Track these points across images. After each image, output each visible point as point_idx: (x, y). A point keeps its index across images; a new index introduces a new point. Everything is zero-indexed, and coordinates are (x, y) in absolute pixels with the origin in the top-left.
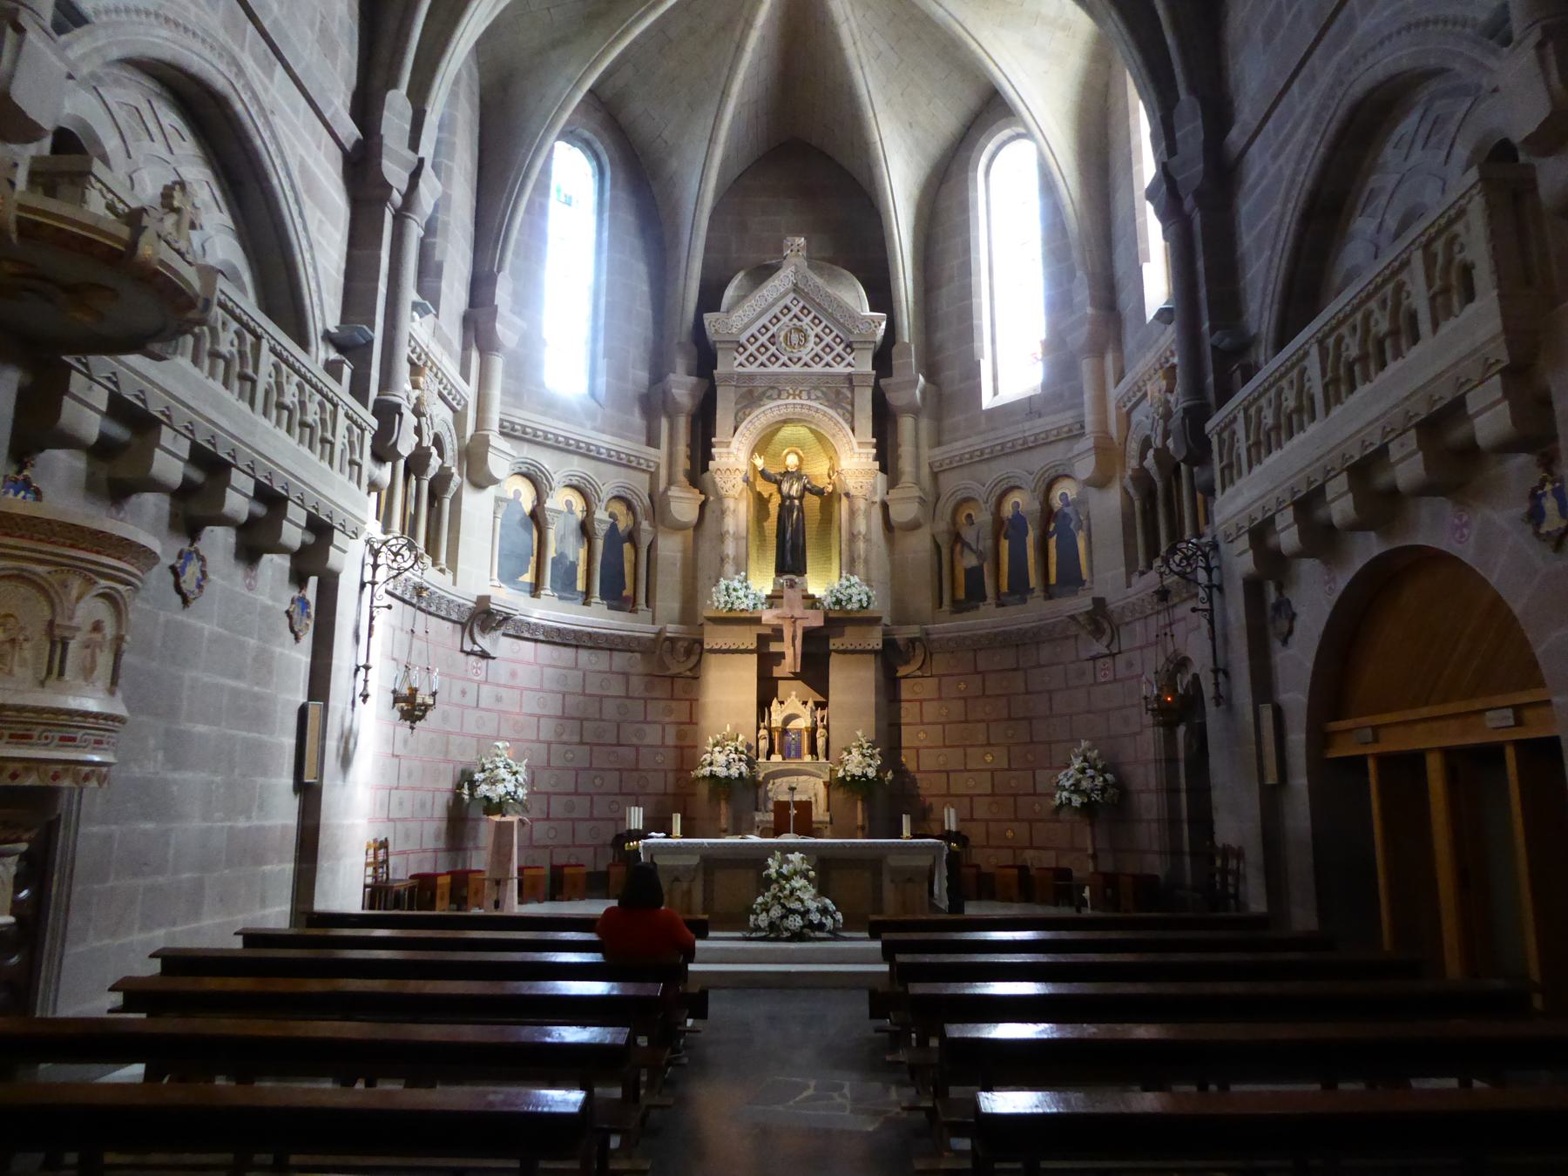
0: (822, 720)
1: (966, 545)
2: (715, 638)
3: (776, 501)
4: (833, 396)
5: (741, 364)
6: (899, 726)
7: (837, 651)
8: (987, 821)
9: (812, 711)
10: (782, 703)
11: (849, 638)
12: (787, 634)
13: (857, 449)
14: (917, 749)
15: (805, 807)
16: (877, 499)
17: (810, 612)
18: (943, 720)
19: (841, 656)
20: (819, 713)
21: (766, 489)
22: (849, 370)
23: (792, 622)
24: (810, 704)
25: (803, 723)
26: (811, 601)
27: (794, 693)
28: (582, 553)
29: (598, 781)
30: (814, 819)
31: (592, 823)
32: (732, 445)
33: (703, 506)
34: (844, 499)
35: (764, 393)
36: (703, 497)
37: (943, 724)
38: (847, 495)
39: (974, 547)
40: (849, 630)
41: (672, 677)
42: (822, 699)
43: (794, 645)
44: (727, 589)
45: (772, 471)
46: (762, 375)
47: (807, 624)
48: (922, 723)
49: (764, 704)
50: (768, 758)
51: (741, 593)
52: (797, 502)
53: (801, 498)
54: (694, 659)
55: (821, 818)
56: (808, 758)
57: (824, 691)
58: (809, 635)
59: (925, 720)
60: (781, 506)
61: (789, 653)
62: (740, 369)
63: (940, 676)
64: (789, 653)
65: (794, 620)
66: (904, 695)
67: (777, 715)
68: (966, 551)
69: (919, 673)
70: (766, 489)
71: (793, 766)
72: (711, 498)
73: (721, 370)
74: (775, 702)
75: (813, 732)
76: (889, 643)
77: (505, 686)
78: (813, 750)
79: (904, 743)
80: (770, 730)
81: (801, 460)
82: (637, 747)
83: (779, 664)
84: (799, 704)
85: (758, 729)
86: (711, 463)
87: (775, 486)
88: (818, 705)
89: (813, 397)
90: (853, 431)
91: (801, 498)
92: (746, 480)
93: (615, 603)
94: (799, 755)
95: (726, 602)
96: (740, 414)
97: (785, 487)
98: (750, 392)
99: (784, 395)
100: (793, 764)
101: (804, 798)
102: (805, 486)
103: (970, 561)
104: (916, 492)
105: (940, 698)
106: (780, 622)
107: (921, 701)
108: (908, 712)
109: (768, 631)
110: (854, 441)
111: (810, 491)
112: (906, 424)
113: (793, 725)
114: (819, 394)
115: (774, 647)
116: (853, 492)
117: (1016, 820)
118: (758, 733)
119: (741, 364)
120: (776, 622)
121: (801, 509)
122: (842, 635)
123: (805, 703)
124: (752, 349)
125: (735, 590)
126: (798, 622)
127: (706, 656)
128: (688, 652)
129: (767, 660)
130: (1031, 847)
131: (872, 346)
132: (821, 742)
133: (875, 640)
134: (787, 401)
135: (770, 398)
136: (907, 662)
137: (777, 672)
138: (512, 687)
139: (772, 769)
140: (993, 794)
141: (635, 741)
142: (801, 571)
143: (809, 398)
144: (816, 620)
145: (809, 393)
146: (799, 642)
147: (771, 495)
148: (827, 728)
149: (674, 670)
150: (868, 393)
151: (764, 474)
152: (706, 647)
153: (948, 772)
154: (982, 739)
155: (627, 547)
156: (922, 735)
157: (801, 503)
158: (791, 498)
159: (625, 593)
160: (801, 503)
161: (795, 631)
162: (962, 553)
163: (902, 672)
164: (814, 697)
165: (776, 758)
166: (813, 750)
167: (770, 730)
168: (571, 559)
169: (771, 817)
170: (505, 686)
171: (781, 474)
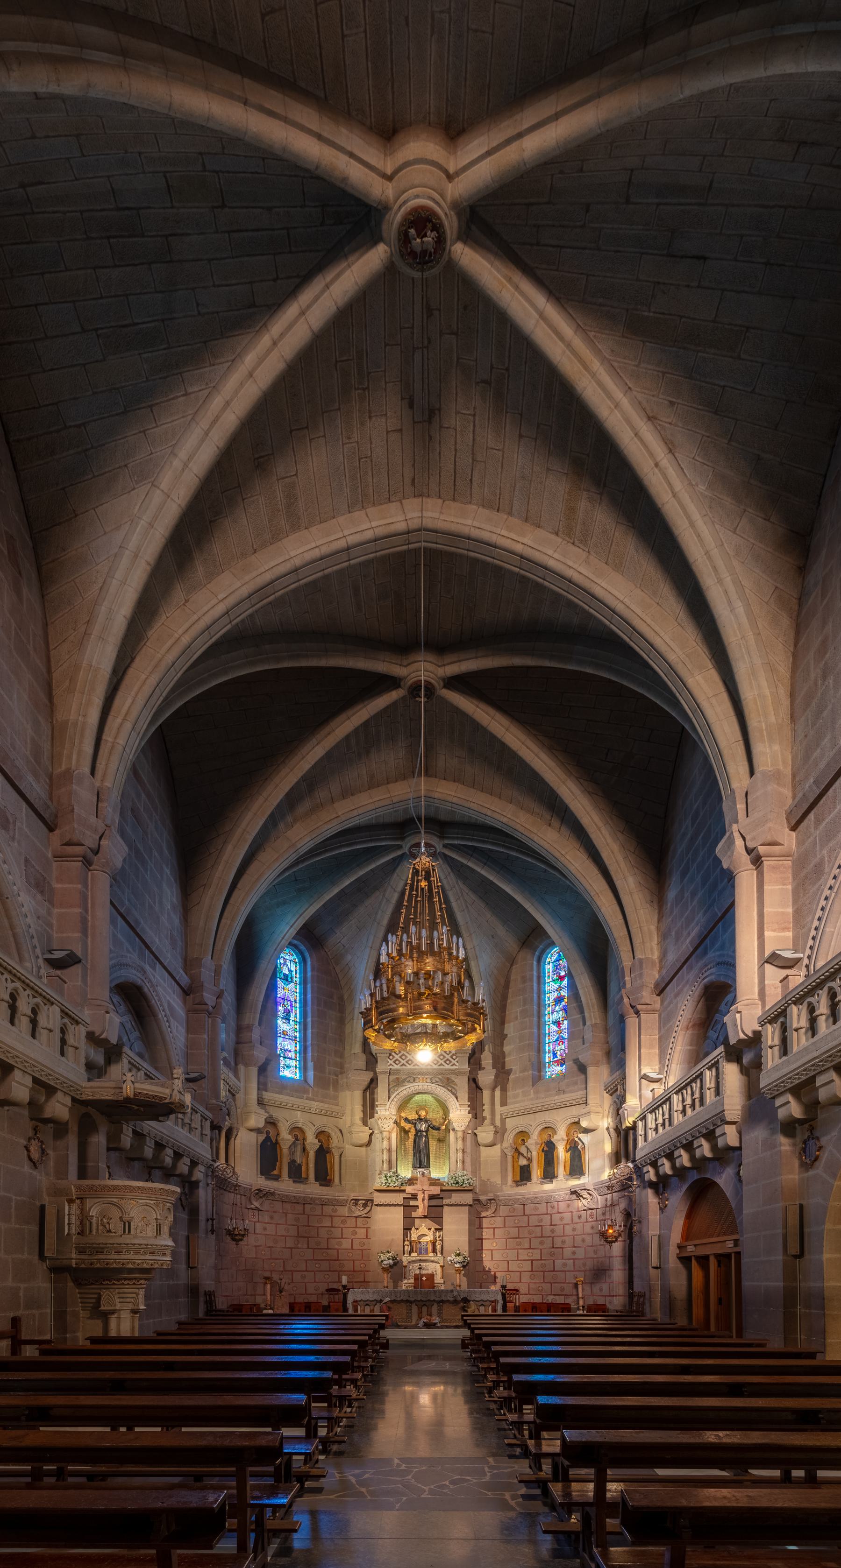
0: (439, 1237)
1: (520, 1153)
2: (379, 1198)
3: (413, 1131)
4: (446, 1081)
5: (391, 1065)
6: (482, 1239)
7: (447, 1205)
8: (529, 1283)
9: (434, 1233)
10: (417, 1229)
11: (456, 1198)
12: (420, 1197)
13: (459, 1108)
14: (492, 1251)
15: (431, 1277)
16: (470, 1132)
17: (432, 1188)
18: (506, 1237)
19: (449, 1208)
20: (437, 1234)
21: (407, 1126)
22: (454, 1067)
23: (423, 1190)
24: (433, 1229)
25: (429, 1238)
26: (434, 1182)
27: (424, 1225)
28: (304, 1161)
29: (317, 1266)
30: (435, 1282)
31: (315, 1285)
32: (388, 1106)
33: (371, 1135)
34: (451, 1131)
35: (405, 1080)
36: (371, 1131)
37: (506, 1239)
38: (454, 1130)
39: (525, 1155)
40: (454, 1195)
41: (356, 1217)
42: (438, 1227)
43: (423, 1203)
44: (386, 1176)
45: (410, 1117)
46: (403, 1069)
47: (431, 1193)
48: (494, 1238)
49: (407, 1230)
50: (410, 1254)
51: (394, 1179)
52: (424, 1133)
53: (427, 1131)
54: (368, 1209)
55: (439, 1282)
56: (431, 1254)
57: (440, 1223)
58: (432, 1197)
59: (496, 1237)
60: (416, 1135)
61: (421, 1206)
62: (391, 1067)
63: (505, 1217)
64: (421, 1206)
65: (424, 1191)
66: (485, 1225)
67: (414, 1235)
68: (521, 1157)
69: (493, 1215)
70: (407, 1126)
71: (424, 1258)
72: (376, 1132)
73: (380, 1067)
74: (413, 1228)
75: (434, 1243)
76: (477, 1201)
77: (268, 1223)
78: (434, 1250)
79: (484, 1248)
80: (411, 1242)
81: (427, 1113)
82: (338, 1250)
83: (415, 1211)
84: (427, 1230)
85: (404, 1241)
86: (375, 1115)
87: (412, 1126)
88: (436, 1229)
89: (434, 1081)
90: (457, 1098)
91: (427, 1131)
92: (396, 1122)
93: (323, 1183)
94: (426, 1253)
95: (386, 1183)
96: (392, 1090)
97: (418, 1126)
98: (398, 1079)
99: (417, 1080)
100: (423, 1257)
101: (430, 1272)
102: (429, 1126)
103: (523, 1162)
104: (492, 1128)
105: (505, 1227)
106: (416, 1192)
107: (494, 1228)
108: (487, 1234)
109: (410, 1196)
110: (457, 1103)
111: (432, 1128)
112: (486, 1094)
113: (424, 1239)
114: (437, 1080)
115: (412, 1203)
116: (456, 1129)
117: (544, 1282)
118: (404, 1241)
119: (391, 1065)
120: (413, 1192)
121: (427, 1137)
122: (450, 1198)
123: (430, 1229)
124: (397, 1057)
125: (390, 1177)
126: (426, 1192)
127: (374, 1207)
128: (365, 1205)
129: (408, 1208)
130: (552, 1294)
131: (468, 1055)
132: (438, 1247)
133: (468, 1198)
134: (419, 1084)
135: (409, 1082)
136: (487, 1210)
137: (414, 1214)
138: (271, 1223)
139: (412, 1259)
140: (532, 1271)
141: (337, 1247)
142: (428, 1166)
143: (432, 1082)
144: (436, 1190)
145: (431, 1079)
146: (426, 1201)
147: (410, 1128)
148: (442, 1240)
149: (357, 1214)
150: (465, 1079)
151: (406, 1120)
152: (375, 1203)
153: (508, 1261)
154: (527, 1245)
155: (328, 1155)
156: (494, 1244)
157: (427, 1134)
158: (421, 1131)
159: (328, 1178)
160: (427, 1134)
161: (424, 1197)
162: (518, 1159)
163: (483, 1214)
164: (434, 1226)
165: (414, 1254)
166: (434, 1250)
167: (411, 1242)
168: (298, 1162)
169: (412, 1281)
170: (268, 1223)
171: (415, 1120)
